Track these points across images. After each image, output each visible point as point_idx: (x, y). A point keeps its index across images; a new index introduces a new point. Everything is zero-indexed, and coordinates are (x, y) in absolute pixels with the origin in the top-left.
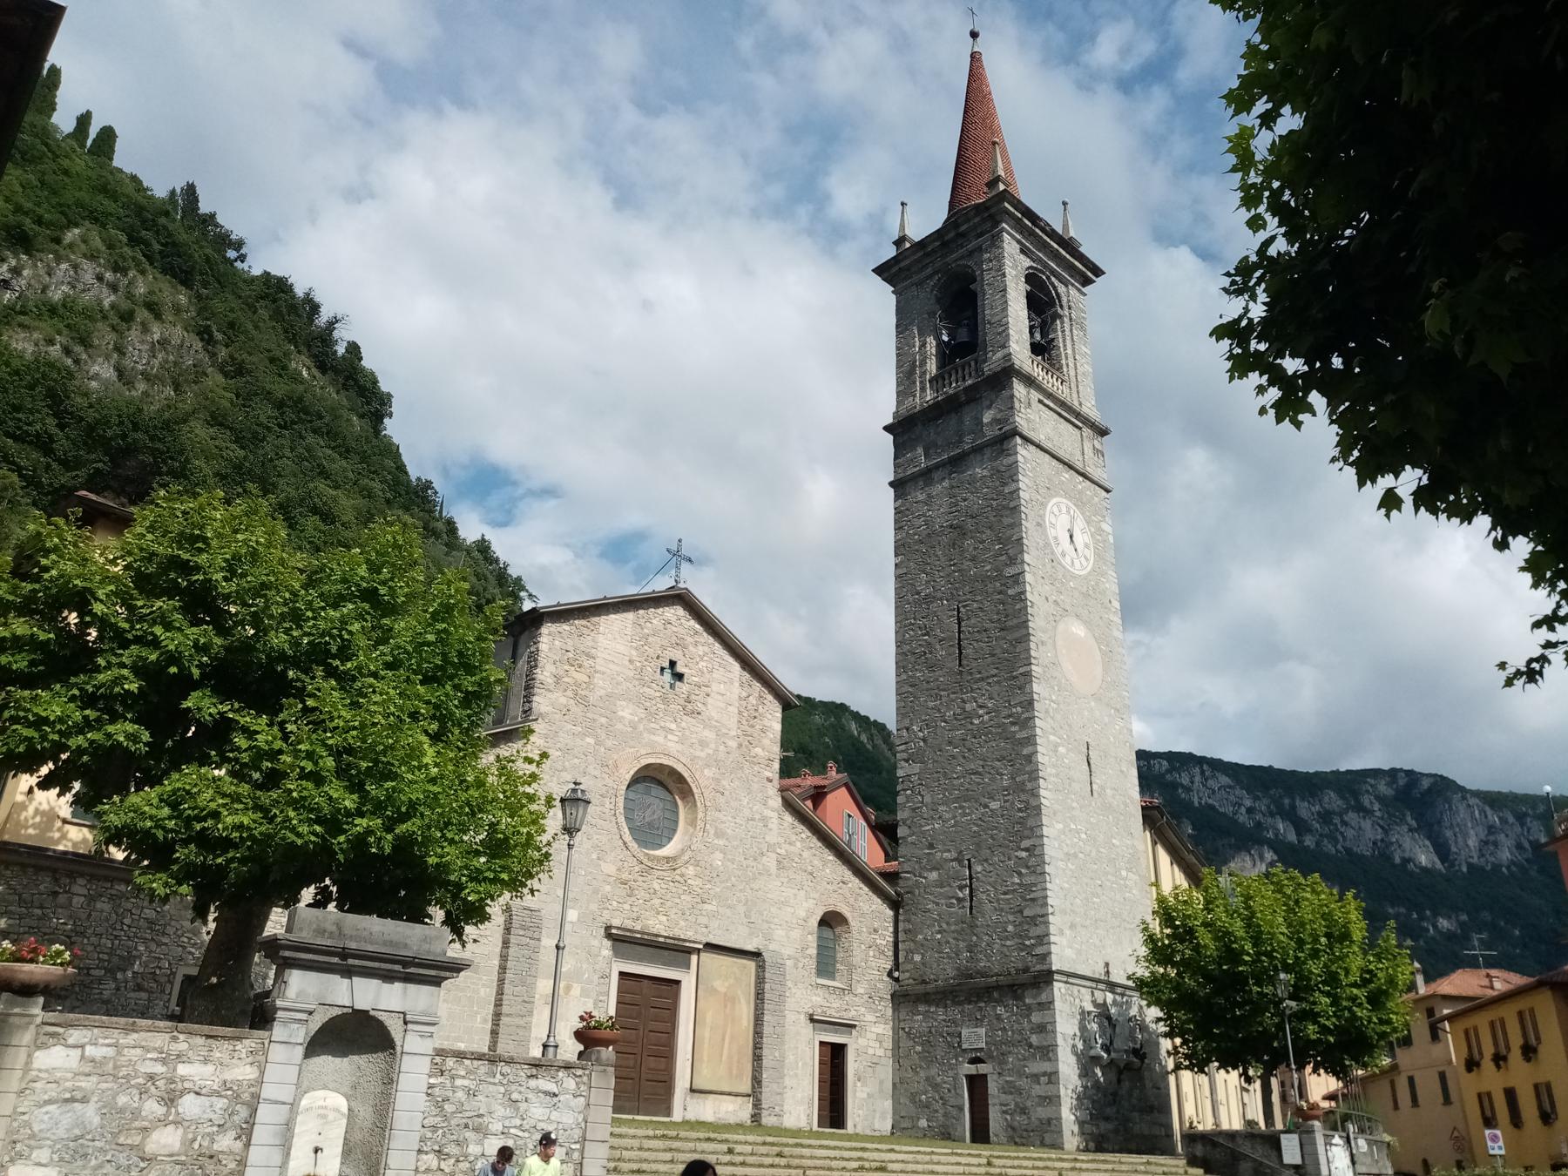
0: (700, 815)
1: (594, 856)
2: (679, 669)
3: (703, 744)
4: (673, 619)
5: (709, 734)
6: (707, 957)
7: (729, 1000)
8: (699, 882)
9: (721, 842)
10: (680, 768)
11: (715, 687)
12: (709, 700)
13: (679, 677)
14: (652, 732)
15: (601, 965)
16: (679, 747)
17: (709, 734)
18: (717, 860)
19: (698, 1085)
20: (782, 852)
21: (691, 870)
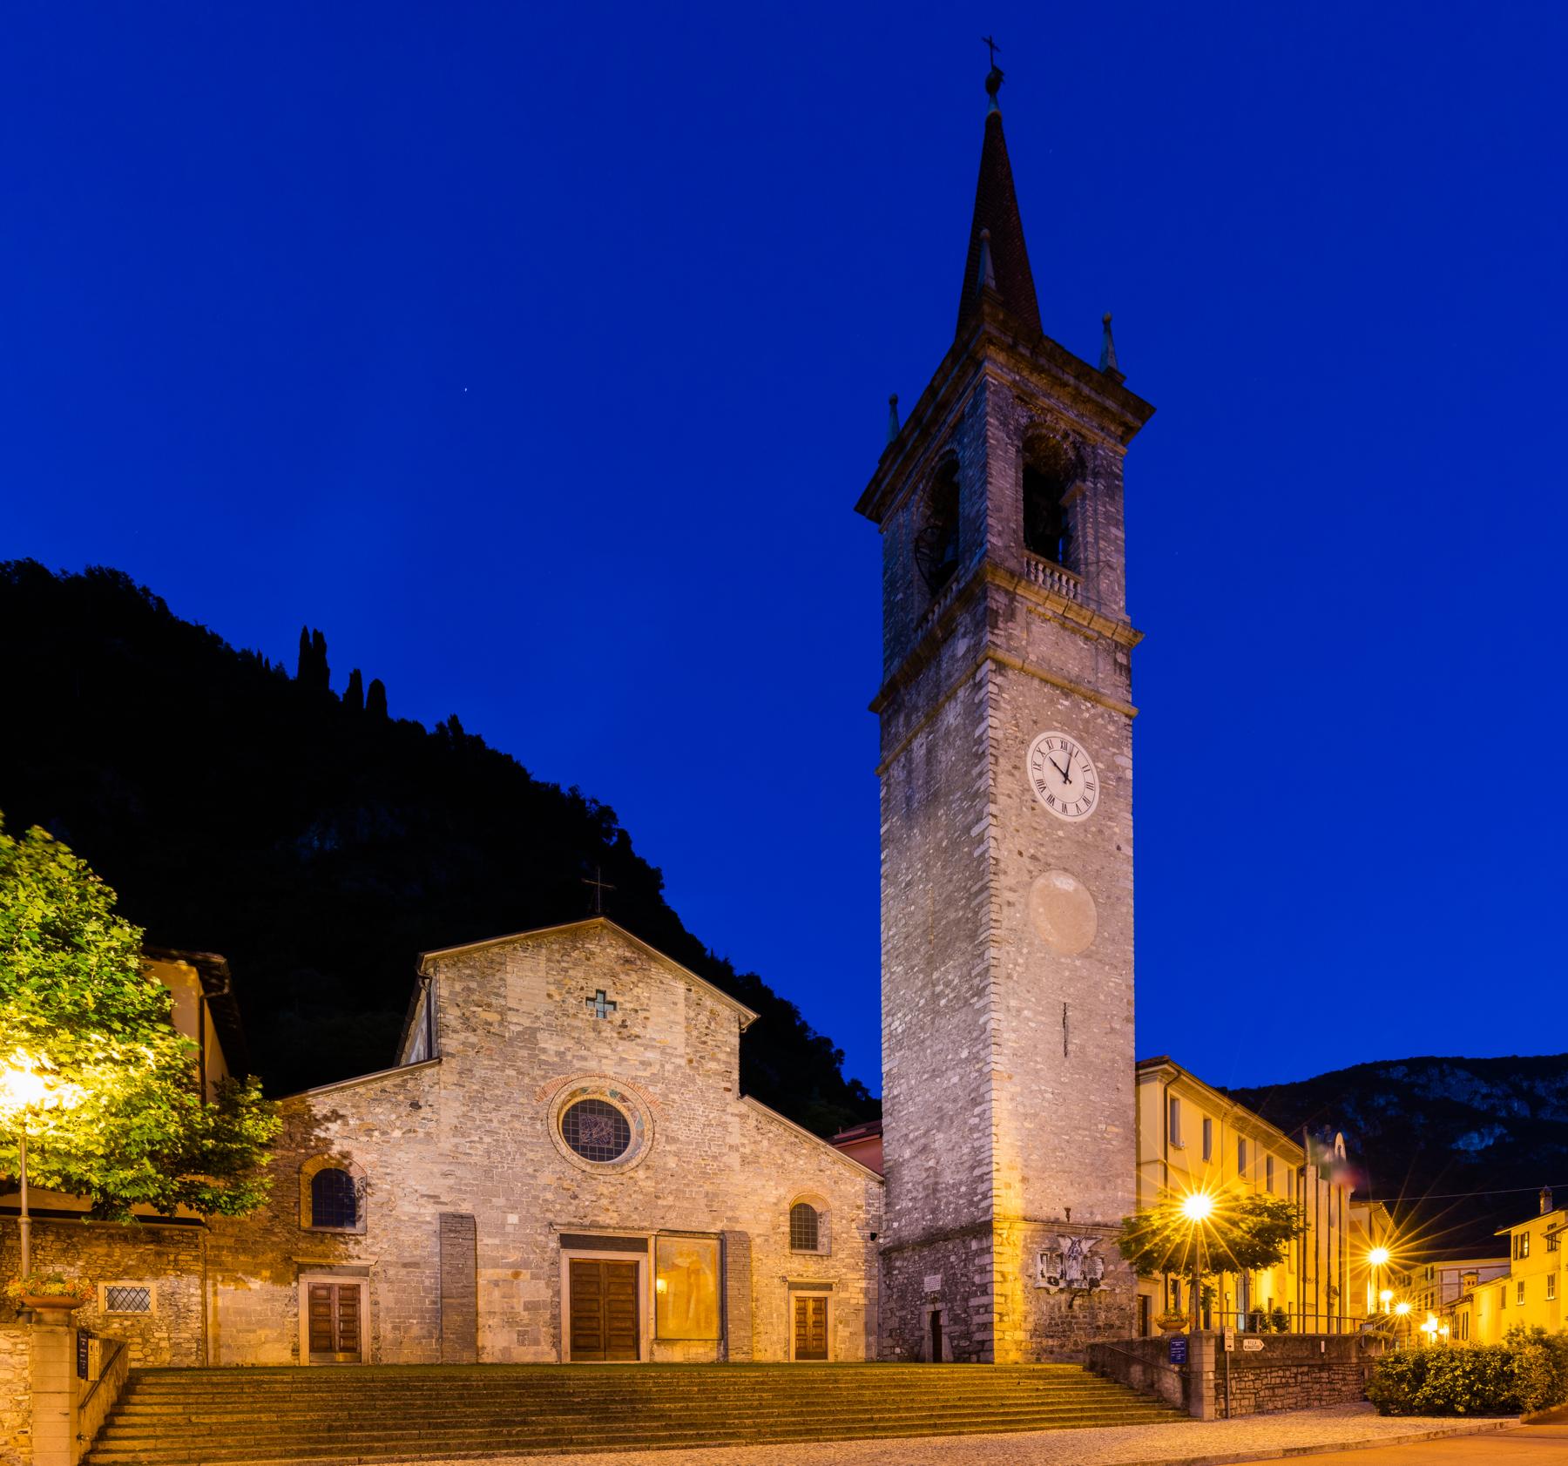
0: (648, 1126)
1: (530, 1170)
2: (611, 996)
3: (646, 1064)
4: (597, 950)
5: (651, 1055)
6: (665, 1241)
7: (694, 1272)
8: (650, 1183)
9: (673, 1148)
10: (620, 1088)
11: (654, 1009)
12: (649, 1024)
13: (614, 1003)
14: (584, 1059)
15: (549, 1254)
16: (618, 1070)
17: (651, 1055)
18: (672, 1163)
19: (663, 1334)
20: (747, 1151)
21: (641, 1174)
